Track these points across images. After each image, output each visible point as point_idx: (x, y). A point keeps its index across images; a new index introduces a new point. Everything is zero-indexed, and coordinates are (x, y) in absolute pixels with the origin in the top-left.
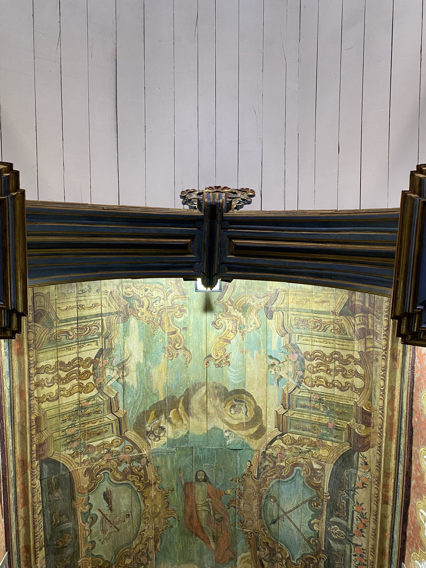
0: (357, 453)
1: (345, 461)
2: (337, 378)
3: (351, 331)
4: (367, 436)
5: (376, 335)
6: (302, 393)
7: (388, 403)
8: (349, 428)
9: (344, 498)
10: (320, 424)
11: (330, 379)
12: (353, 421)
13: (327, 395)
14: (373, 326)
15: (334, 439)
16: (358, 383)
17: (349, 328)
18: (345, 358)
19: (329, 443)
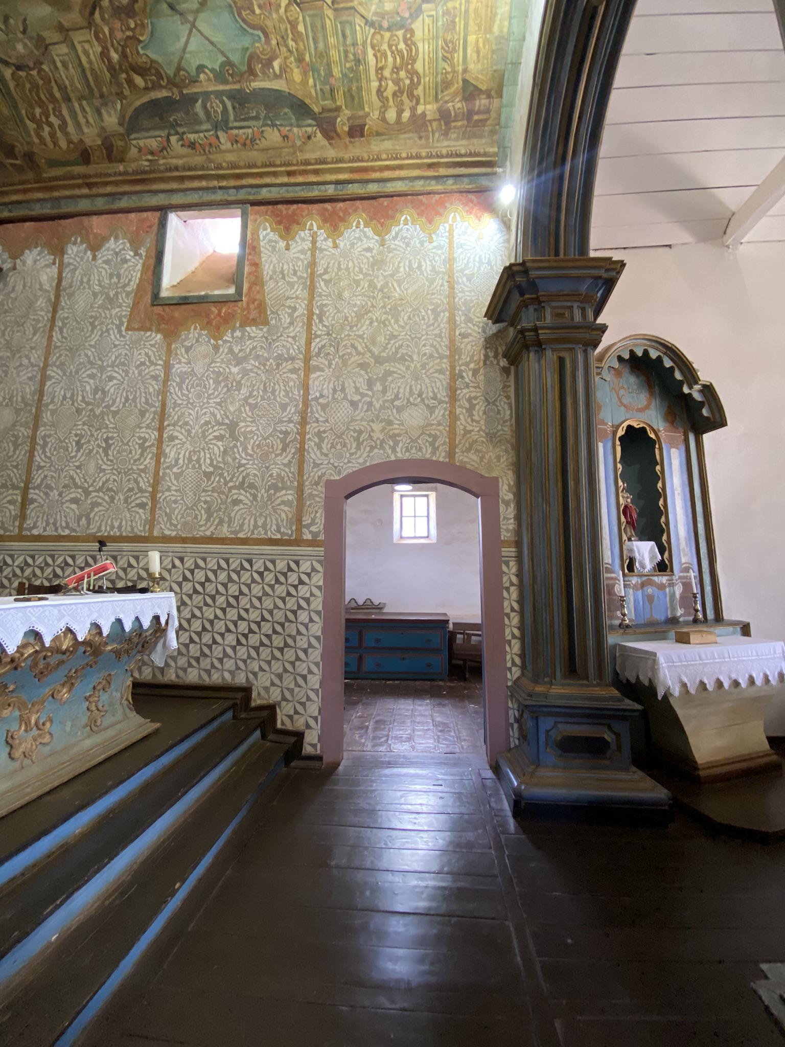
0: (314, 123)
1: (301, 109)
2: (390, 83)
3: (447, 98)
4: (338, 135)
5: (446, 134)
6: (362, 32)
7: (387, 166)
8: (338, 109)
9: (257, 112)
10: (329, 65)
11: (387, 73)
12: (348, 113)
13: (366, 70)
14: (455, 127)
15: (318, 87)
16: (391, 115)
17: (449, 94)
18: (415, 93)
19: (311, 81)
